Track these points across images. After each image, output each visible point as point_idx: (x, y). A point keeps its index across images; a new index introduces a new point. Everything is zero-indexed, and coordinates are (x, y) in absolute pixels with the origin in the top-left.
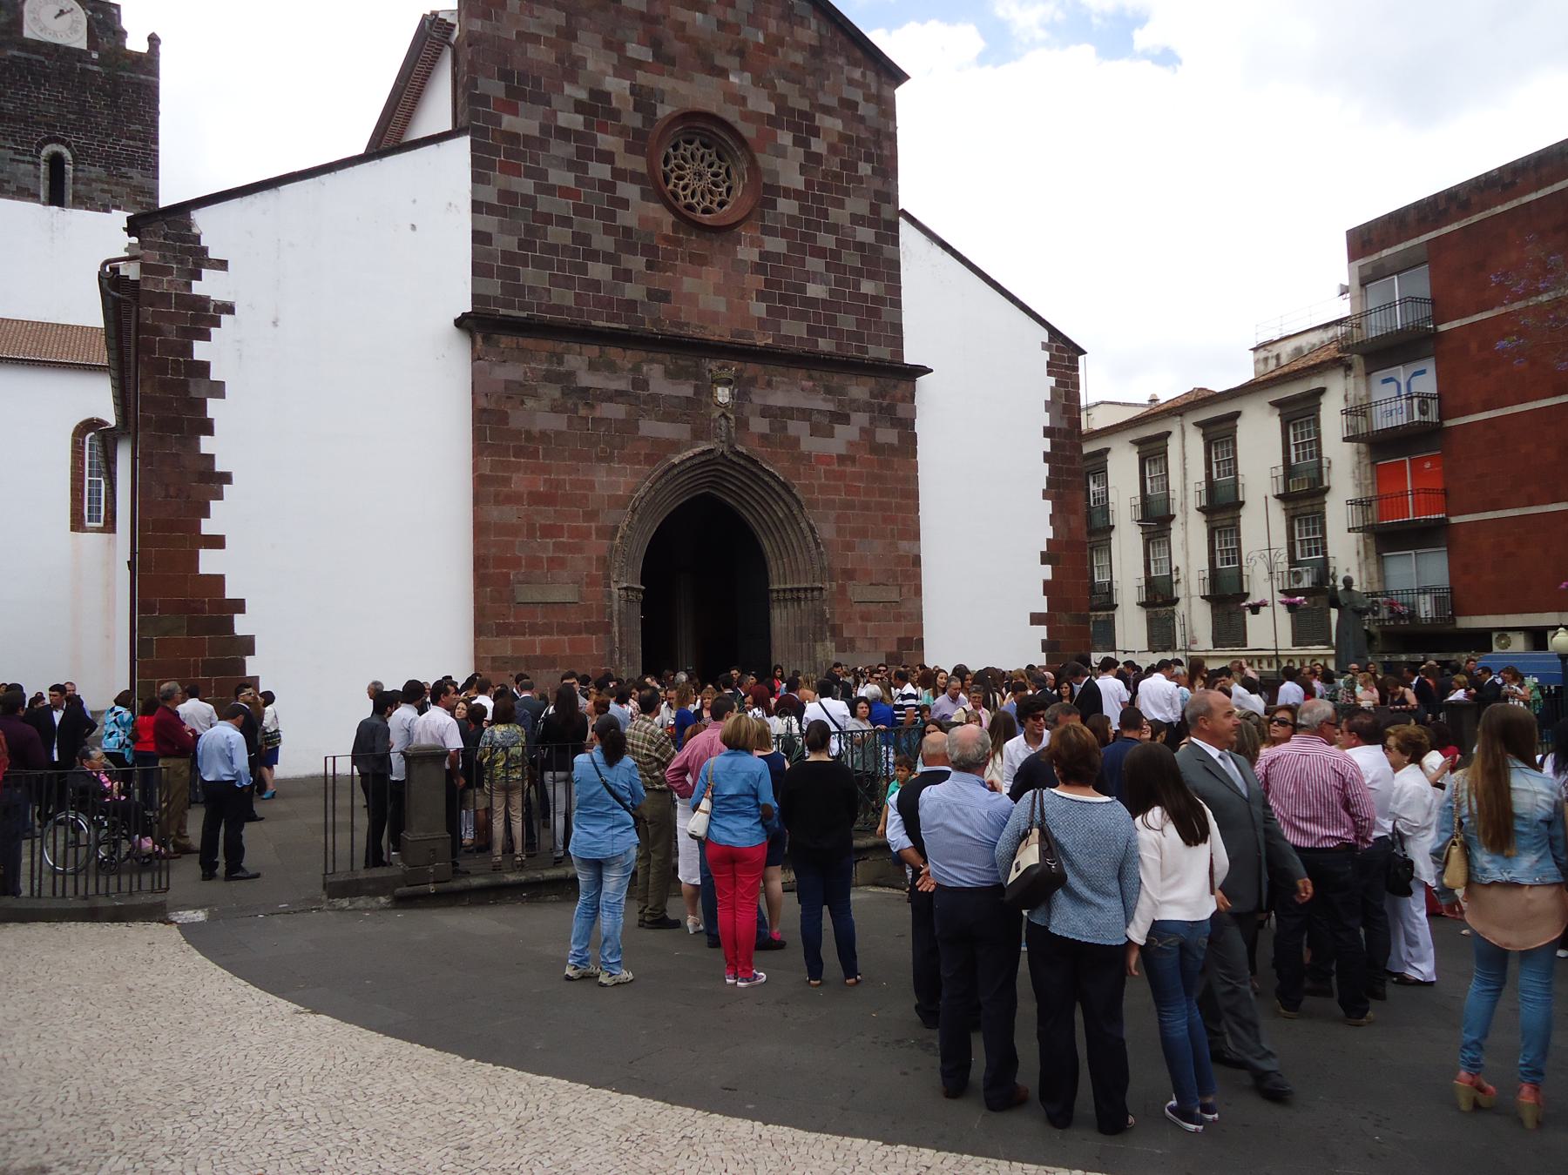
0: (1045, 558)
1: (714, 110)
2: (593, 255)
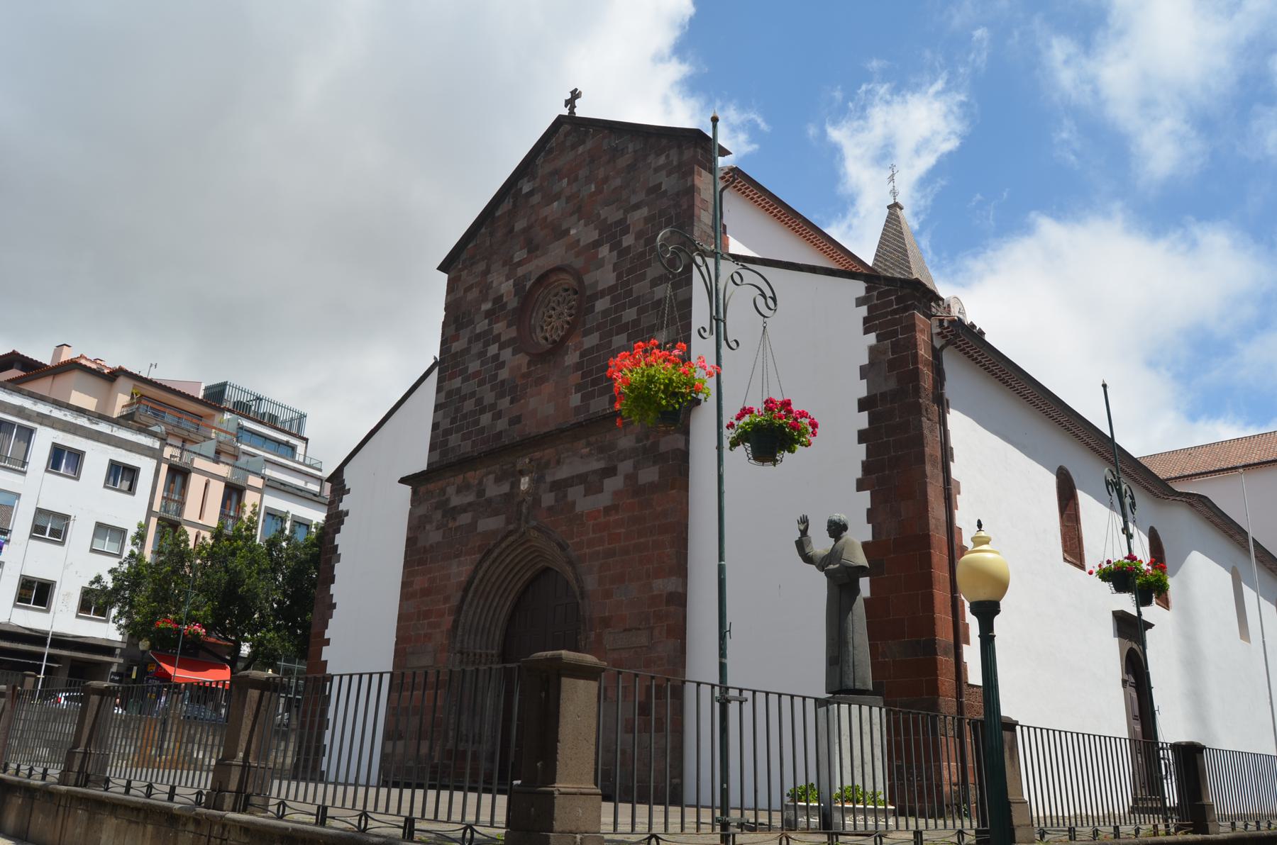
1: (558, 263)
2: (483, 411)
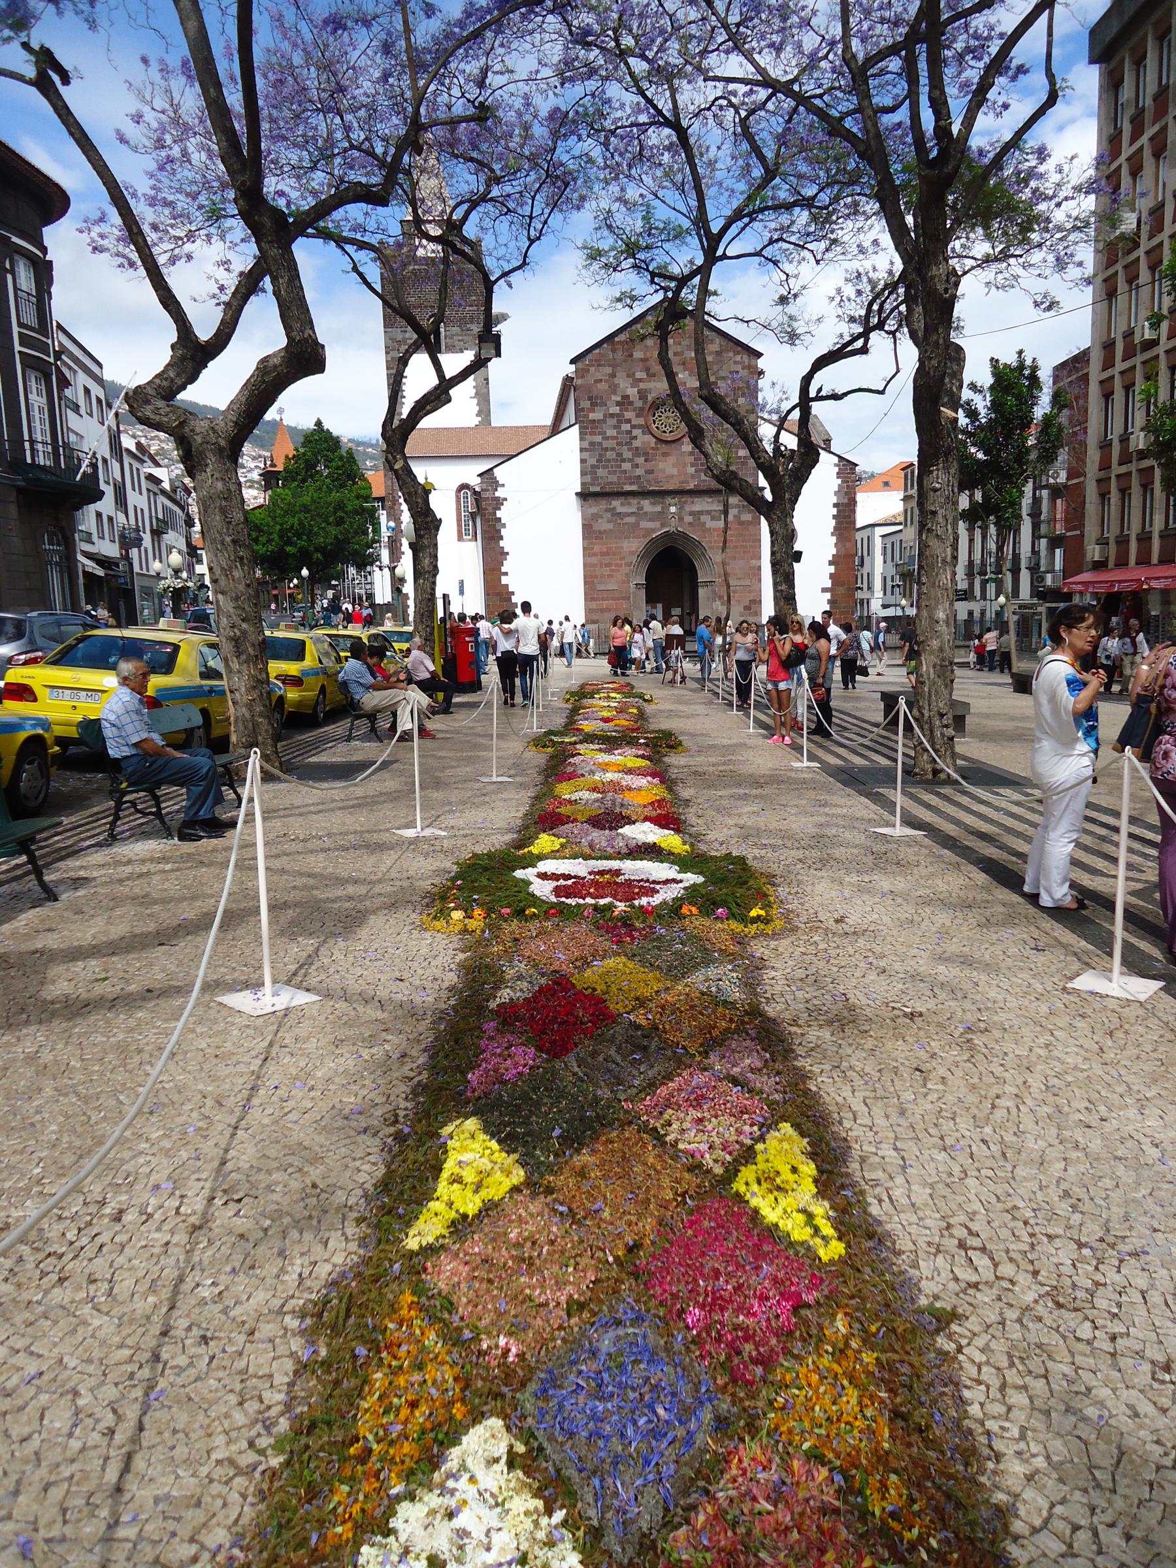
0: (830, 563)
2: (624, 460)
